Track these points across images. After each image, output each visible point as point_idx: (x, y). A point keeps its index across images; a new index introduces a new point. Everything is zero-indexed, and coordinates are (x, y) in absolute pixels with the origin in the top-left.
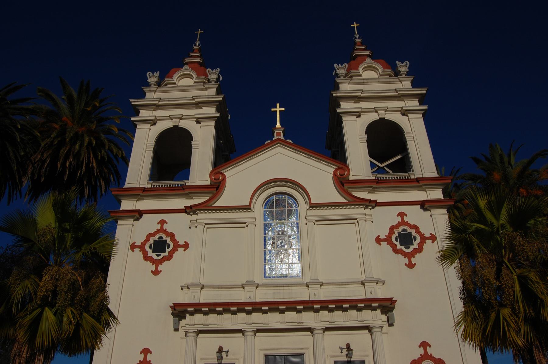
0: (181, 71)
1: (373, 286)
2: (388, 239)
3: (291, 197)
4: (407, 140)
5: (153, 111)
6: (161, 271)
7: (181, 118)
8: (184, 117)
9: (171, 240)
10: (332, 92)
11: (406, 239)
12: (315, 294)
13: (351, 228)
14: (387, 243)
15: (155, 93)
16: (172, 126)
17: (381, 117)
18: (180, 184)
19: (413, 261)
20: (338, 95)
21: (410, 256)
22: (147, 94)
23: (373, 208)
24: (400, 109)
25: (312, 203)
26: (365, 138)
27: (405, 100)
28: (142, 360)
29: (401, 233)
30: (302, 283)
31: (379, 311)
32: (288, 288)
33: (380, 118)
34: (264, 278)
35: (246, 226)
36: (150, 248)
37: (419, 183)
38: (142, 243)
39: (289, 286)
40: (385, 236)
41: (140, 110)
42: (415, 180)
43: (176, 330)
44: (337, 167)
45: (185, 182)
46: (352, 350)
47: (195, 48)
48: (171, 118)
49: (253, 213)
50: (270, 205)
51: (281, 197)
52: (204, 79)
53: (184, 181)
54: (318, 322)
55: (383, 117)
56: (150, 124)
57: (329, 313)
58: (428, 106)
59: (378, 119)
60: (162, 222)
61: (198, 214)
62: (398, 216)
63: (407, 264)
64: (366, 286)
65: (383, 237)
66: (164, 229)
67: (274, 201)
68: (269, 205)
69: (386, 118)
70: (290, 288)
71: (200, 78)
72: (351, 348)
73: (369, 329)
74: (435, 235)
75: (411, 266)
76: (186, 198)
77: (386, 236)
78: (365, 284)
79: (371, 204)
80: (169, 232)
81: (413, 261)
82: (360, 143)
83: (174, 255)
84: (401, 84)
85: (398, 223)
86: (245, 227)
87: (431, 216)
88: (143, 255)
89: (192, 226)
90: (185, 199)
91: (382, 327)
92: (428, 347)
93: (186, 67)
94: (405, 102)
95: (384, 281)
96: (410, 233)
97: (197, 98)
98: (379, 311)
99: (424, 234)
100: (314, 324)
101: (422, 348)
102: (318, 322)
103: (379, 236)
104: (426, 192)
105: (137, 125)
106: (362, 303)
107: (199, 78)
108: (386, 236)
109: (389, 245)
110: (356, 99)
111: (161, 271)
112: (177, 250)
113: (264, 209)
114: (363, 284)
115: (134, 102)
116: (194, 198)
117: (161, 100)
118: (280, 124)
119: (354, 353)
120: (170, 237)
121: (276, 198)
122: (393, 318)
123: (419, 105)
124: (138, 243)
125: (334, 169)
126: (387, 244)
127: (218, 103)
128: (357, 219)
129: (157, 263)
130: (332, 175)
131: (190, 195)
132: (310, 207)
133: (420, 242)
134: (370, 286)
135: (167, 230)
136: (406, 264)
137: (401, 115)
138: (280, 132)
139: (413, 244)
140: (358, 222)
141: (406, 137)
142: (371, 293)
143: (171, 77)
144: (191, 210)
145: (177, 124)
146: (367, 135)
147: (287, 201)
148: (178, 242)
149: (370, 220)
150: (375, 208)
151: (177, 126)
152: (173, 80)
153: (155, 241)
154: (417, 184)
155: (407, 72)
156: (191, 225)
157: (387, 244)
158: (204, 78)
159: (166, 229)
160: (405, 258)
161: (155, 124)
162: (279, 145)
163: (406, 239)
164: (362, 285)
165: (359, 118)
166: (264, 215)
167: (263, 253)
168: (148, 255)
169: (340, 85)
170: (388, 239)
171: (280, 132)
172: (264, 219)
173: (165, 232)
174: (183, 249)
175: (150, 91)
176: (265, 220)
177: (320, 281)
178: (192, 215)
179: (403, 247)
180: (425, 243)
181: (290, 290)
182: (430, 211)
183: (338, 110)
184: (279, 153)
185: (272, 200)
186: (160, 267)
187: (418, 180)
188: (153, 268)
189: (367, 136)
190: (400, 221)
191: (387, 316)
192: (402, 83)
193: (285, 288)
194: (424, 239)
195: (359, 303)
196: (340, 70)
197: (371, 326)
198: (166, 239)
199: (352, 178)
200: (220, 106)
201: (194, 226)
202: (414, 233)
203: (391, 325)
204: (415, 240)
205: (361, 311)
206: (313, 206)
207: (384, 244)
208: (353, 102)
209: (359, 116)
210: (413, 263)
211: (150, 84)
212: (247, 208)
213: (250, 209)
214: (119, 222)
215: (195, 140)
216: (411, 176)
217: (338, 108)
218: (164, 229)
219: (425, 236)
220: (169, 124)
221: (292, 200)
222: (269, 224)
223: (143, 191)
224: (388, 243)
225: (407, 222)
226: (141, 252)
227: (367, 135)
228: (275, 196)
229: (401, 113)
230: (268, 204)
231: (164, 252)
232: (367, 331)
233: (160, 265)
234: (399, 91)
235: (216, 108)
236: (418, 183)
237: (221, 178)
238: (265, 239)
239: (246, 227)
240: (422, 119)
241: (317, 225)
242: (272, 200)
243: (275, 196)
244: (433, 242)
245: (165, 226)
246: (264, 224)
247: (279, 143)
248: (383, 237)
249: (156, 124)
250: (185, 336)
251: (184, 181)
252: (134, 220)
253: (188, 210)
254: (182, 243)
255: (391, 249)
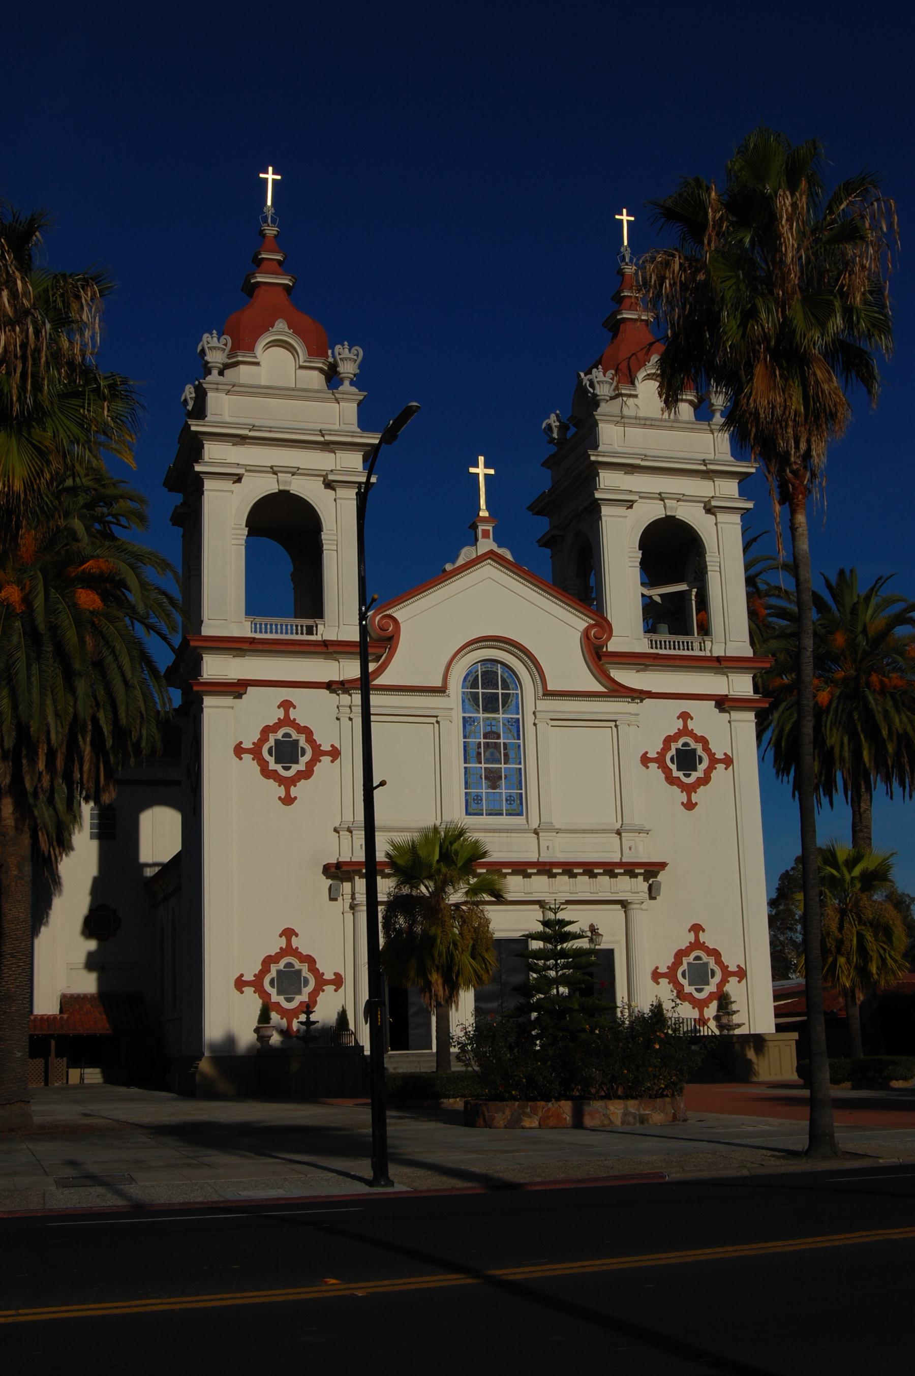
0: (271, 334)
1: (633, 838)
2: (660, 760)
3: (506, 669)
4: (709, 568)
5: (233, 445)
6: (295, 798)
7: (295, 472)
8: (300, 471)
9: (307, 741)
10: (589, 453)
11: (687, 760)
12: (548, 847)
13: (605, 734)
14: (657, 765)
15: (226, 394)
16: (277, 491)
17: (669, 514)
18: (306, 626)
19: (694, 798)
20: (600, 459)
21: (689, 789)
22: (209, 394)
23: (641, 702)
24: (707, 499)
25: (548, 689)
26: (638, 557)
27: (715, 479)
28: (284, 947)
29: (679, 749)
30: (526, 827)
31: (641, 878)
32: (505, 835)
33: (667, 517)
34: (466, 815)
35: (435, 722)
36: (270, 753)
37: (721, 665)
38: (254, 743)
39: (508, 832)
40: (655, 753)
41: (205, 442)
42: (715, 659)
43: (333, 899)
44: (594, 622)
45: (317, 622)
46: (602, 935)
47: (267, 232)
48: (274, 470)
49: (447, 698)
50: (473, 681)
51: (491, 668)
52: (323, 363)
53: (315, 621)
54: (554, 893)
55: (673, 514)
56: (232, 482)
57: (571, 879)
58: (754, 502)
59: (664, 516)
60: (287, 705)
61: (353, 695)
62: (678, 718)
63: (685, 802)
64: (623, 838)
65: (652, 754)
66: (292, 719)
67: (478, 675)
68: (469, 681)
69: (677, 517)
70: (509, 834)
71: (315, 360)
72: (600, 931)
73: (624, 904)
74: (731, 756)
75: (690, 806)
76: (325, 659)
77: (658, 753)
78: (623, 834)
79: (641, 696)
80: (302, 725)
81: (694, 798)
82: (630, 567)
83: (315, 769)
84: (712, 435)
85: (677, 731)
86: (433, 723)
87: (729, 722)
88: (259, 768)
89: (342, 716)
90: (322, 660)
91: (643, 902)
92: (701, 932)
93: (281, 324)
94: (714, 482)
95: (650, 830)
96: (694, 751)
97: (330, 435)
98: (641, 878)
99: (715, 754)
100: (548, 895)
101: (692, 932)
102: (554, 893)
103: (647, 753)
104: (727, 677)
105: (205, 480)
106: (621, 869)
107: (312, 360)
108: (658, 753)
109: (660, 770)
110: (629, 469)
111: (295, 798)
112: (320, 761)
113: (462, 688)
114: (619, 833)
115: (197, 425)
116: (340, 660)
117: (254, 428)
118: (488, 508)
119: (604, 939)
120: (304, 735)
121: (481, 669)
122: (659, 889)
123: (737, 496)
124: (247, 745)
125: (587, 624)
126: (658, 768)
127: (370, 448)
128: (617, 722)
129: (288, 783)
130: (580, 634)
131: (338, 656)
132: (544, 695)
133: (708, 767)
134: (630, 838)
135: (297, 722)
136: (682, 803)
137: (704, 511)
138: (489, 530)
139: (695, 770)
140: (616, 726)
141: (708, 563)
142: (630, 849)
143: (251, 348)
144: (341, 687)
145: (287, 488)
146: (641, 551)
147: (501, 676)
148: (320, 745)
149: (636, 723)
150: (644, 701)
151: (289, 491)
152: (256, 357)
153: (277, 741)
154: (717, 665)
155: (725, 407)
156: (340, 716)
157: (658, 768)
158: (323, 361)
159: (295, 720)
160: (682, 792)
161: (238, 479)
162: (489, 561)
163: (687, 760)
164: (616, 835)
165: (629, 510)
166: (463, 701)
167: (463, 771)
168: (270, 768)
169: (600, 425)
170: (660, 760)
171: (489, 530)
172: (463, 709)
173: (293, 724)
174: (330, 758)
175: (217, 389)
176: (464, 712)
177: (557, 827)
178: (341, 695)
179: (680, 774)
180: (715, 768)
181: (509, 838)
182: (730, 714)
183: (598, 495)
184: (490, 578)
185: (476, 672)
186: (294, 792)
187: (718, 659)
188: (282, 792)
189: (642, 554)
190: (681, 728)
191: (648, 885)
192: (713, 434)
193: (502, 834)
194: (714, 761)
195: (618, 867)
196: (602, 385)
197: (629, 901)
198: (298, 738)
199: (613, 646)
200: (371, 457)
201: (346, 717)
202: (700, 751)
203: (652, 898)
204: (700, 762)
205: (617, 877)
206: (548, 694)
207: (653, 766)
208: (623, 472)
209: (631, 507)
210: (694, 802)
211: (209, 365)
212: (441, 690)
213: (444, 692)
214: (205, 700)
215: (327, 530)
216: (706, 642)
217: (597, 489)
218: (292, 719)
219: (716, 756)
220: (268, 486)
221: (510, 674)
222: (470, 717)
223: (250, 644)
224: (659, 765)
225: (692, 730)
226: (255, 761)
227: (641, 551)
228: (481, 665)
229: (704, 508)
230: (471, 681)
231: (297, 762)
232: (619, 907)
233: (292, 787)
234: (710, 464)
235: (363, 455)
236: (718, 664)
237: (390, 629)
238: (465, 747)
239: (435, 724)
240: (740, 526)
241: (552, 726)
242: (476, 672)
243: (479, 664)
244: (726, 769)
245: (293, 714)
246: (464, 718)
247: (490, 558)
248: (652, 754)
249: (243, 479)
250: (349, 910)
251: (315, 621)
252: (234, 698)
253: (334, 687)
254: (326, 747)
255: (664, 776)
